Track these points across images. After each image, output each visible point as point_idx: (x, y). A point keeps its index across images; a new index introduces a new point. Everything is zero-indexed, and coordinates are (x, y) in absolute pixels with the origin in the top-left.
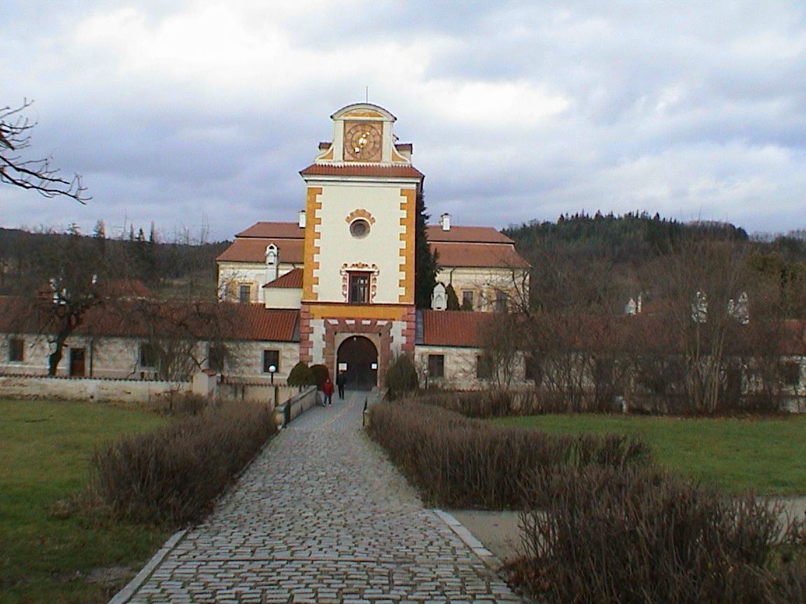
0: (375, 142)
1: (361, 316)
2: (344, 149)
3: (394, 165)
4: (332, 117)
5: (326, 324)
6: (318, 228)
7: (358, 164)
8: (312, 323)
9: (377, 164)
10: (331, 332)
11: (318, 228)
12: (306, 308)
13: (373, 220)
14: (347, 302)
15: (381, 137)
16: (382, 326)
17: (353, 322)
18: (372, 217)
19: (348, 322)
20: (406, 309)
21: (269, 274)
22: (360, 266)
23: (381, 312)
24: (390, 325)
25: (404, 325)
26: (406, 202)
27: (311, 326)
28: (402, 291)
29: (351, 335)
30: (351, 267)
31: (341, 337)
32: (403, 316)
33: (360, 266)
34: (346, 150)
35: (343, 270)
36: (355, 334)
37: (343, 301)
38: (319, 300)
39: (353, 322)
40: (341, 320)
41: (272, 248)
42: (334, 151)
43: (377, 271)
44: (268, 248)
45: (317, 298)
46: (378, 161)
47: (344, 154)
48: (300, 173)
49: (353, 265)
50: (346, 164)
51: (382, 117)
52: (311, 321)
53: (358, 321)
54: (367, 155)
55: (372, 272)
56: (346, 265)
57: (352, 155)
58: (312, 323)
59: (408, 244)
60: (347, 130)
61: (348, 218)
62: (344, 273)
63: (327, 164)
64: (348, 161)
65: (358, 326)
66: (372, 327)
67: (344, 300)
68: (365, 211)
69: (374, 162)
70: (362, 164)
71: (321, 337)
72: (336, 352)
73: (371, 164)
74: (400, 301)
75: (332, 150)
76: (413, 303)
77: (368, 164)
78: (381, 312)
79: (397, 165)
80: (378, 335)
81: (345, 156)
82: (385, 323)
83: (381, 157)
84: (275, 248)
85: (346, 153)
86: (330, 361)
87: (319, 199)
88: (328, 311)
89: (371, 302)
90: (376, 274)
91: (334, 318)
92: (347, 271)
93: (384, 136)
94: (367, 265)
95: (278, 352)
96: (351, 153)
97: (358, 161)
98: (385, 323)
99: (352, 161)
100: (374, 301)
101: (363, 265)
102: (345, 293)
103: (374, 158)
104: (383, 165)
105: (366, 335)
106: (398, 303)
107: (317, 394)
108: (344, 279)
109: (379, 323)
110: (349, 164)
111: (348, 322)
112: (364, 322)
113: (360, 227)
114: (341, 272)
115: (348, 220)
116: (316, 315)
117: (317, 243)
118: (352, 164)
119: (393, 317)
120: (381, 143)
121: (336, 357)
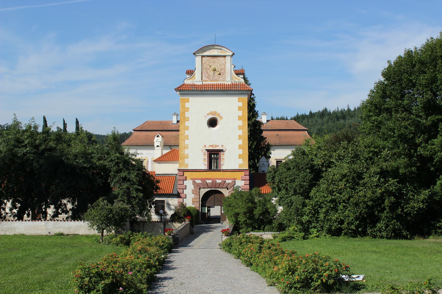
1: (215, 177)
4: (194, 54)
5: (194, 183)
7: (212, 83)
10: (198, 187)
13: (221, 117)
14: (206, 169)
15: (225, 66)
17: (210, 181)
18: (220, 116)
21: (157, 153)
22: (214, 146)
26: (241, 106)
28: (241, 161)
29: (209, 189)
31: (203, 191)
32: (242, 177)
37: (204, 169)
38: (190, 168)
39: (210, 181)
40: (203, 180)
41: (158, 136)
44: (156, 137)
45: (188, 166)
48: (175, 89)
49: (210, 146)
51: (225, 53)
56: (205, 146)
57: (207, 77)
59: (244, 132)
62: (204, 151)
64: (205, 81)
65: (214, 183)
68: (216, 112)
69: (221, 81)
70: (214, 83)
71: (191, 192)
76: (247, 168)
77: (218, 83)
82: (230, 181)
83: (225, 77)
85: (203, 76)
88: (195, 175)
89: (221, 169)
91: (198, 179)
92: (206, 150)
94: (218, 146)
96: (207, 76)
97: (211, 81)
99: (207, 81)
100: (223, 168)
101: (216, 146)
103: (220, 79)
104: (226, 83)
105: (219, 189)
108: (204, 154)
109: (227, 181)
111: (208, 181)
112: (219, 181)
113: (213, 123)
114: (202, 150)
117: (187, 133)
119: (235, 177)
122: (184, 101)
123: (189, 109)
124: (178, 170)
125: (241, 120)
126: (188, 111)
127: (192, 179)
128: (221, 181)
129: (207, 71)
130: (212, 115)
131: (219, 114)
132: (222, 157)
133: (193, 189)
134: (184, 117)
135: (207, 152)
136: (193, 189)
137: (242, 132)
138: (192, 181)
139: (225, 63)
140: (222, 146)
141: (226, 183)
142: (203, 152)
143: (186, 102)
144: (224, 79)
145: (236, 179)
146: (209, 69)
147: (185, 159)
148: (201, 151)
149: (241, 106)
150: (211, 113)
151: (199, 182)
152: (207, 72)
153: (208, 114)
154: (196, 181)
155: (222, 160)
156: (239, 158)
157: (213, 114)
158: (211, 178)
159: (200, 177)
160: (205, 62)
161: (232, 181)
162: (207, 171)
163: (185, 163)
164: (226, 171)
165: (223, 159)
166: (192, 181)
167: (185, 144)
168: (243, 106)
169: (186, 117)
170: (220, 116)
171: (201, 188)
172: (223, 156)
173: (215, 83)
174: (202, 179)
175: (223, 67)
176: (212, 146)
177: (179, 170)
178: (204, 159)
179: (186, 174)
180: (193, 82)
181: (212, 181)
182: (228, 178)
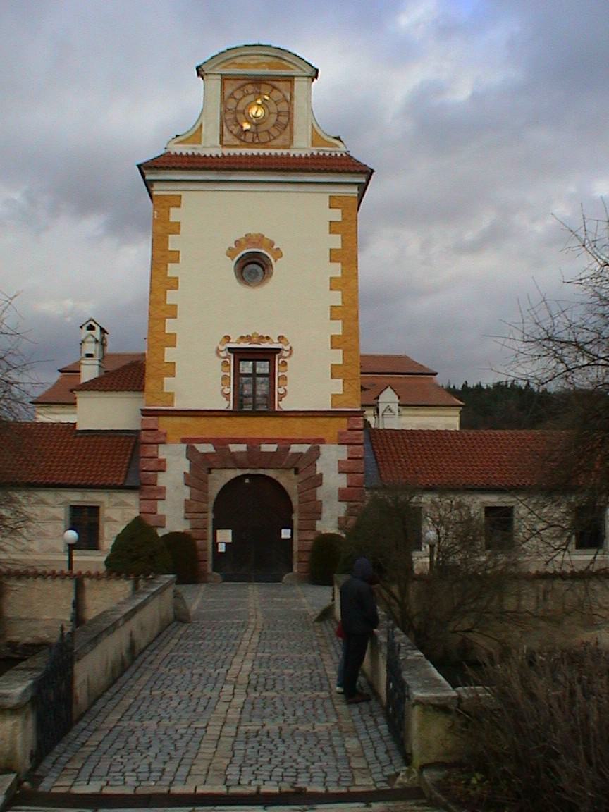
0: (279, 114)
1: (258, 436)
2: (222, 126)
3: (315, 153)
5: (191, 453)
6: (170, 355)
7: (249, 151)
8: (164, 452)
9: (285, 152)
11: (170, 355)
12: (151, 422)
13: (278, 254)
14: (231, 408)
15: (290, 104)
16: (301, 453)
17: (243, 448)
18: (275, 247)
19: (234, 448)
20: (344, 421)
23: (298, 428)
24: (315, 454)
25: (341, 453)
27: (161, 457)
28: (337, 386)
29: (239, 473)
30: (238, 342)
32: (341, 434)
33: (255, 339)
34: (225, 128)
35: (222, 348)
36: (248, 471)
37: (223, 408)
38: (178, 405)
39: (243, 448)
40: (221, 443)
42: (203, 130)
43: (288, 348)
46: (284, 147)
47: (222, 135)
49: (242, 337)
50: (226, 152)
51: (290, 68)
52: (161, 447)
53: (253, 443)
54: (264, 137)
55: (279, 350)
56: (228, 338)
57: (237, 136)
58: (164, 452)
60: (227, 93)
61: (230, 249)
62: (224, 354)
63: (190, 153)
65: (254, 456)
66: (280, 459)
67: (224, 404)
68: (263, 236)
70: (255, 151)
71: (181, 479)
72: (210, 505)
73: (273, 152)
74: (332, 407)
75: (201, 126)
77: (267, 152)
78: (298, 428)
79: (321, 154)
80: (292, 471)
81: (224, 139)
82: (304, 448)
83: (292, 138)
84: (98, 329)
85: (226, 133)
86: (199, 525)
87: (175, 215)
89: (277, 409)
90: (285, 354)
92: (229, 349)
93: (295, 102)
94: (268, 338)
95: (97, 508)
96: (235, 132)
97: (248, 147)
98: (304, 448)
99: (236, 146)
100: (285, 405)
101: (261, 337)
102: (227, 391)
103: (275, 143)
104: (294, 152)
105: (270, 473)
106: (330, 409)
107: (177, 595)
108: (225, 364)
109: (295, 448)
110: (232, 151)
111: (234, 448)
112: (266, 448)
114: (218, 351)
115: (231, 253)
116: (170, 436)
118: (237, 151)
119: (320, 436)
120: (290, 115)
121: (211, 516)
122: (166, 204)
123: (179, 226)
124: (142, 410)
125: (339, 262)
126: (178, 233)
127: (184, 441)
128: (276, 446)
129: (239, 119)
130: (255, 244)
131: (272, 244)
132: (280, 374)
133: (188, 471)
134: (165, 249)
135: (232, 355)
136: (188, 471)
137: (342, 298)
138: (185, 445)
139: (292, 97)
140: (281, 338)
141: (293, 454)
142: (219, 356)
143: (172, 206)
144: (287, 143)
145: (322, 441)
146: (244, 114)
147: (166, 379)
148: (214, 354)
149: (340, 220)
150: (249, 239)
151: (208, 448)
152: (237, 121)
153: (237, 243)
154: (195, 445)
155: (281, 381)
156: (333, 377)
157: (254, 243)
158: (244, 439)
159: (208, 435)
160: (232, 94)
161: (309, 446)
162: (231, 414)
163: (165, 391)
164: (293, 414)
165: (284, 378)
166: (185, 445)
167: (164, 331)
168: (344, 219)
169: (171, 251)
170: (275, 247)
171: (213, 468)
172: (282, 368)
173: (261, 152)
174: (218, 440)
175: (283, 107)
176: (249, 338)
177: (145, 413)
178: (224, 378)
179: (165, 423)
180: (194, 148)
181: (248, 448)
182: (297, 437)
